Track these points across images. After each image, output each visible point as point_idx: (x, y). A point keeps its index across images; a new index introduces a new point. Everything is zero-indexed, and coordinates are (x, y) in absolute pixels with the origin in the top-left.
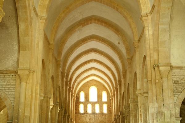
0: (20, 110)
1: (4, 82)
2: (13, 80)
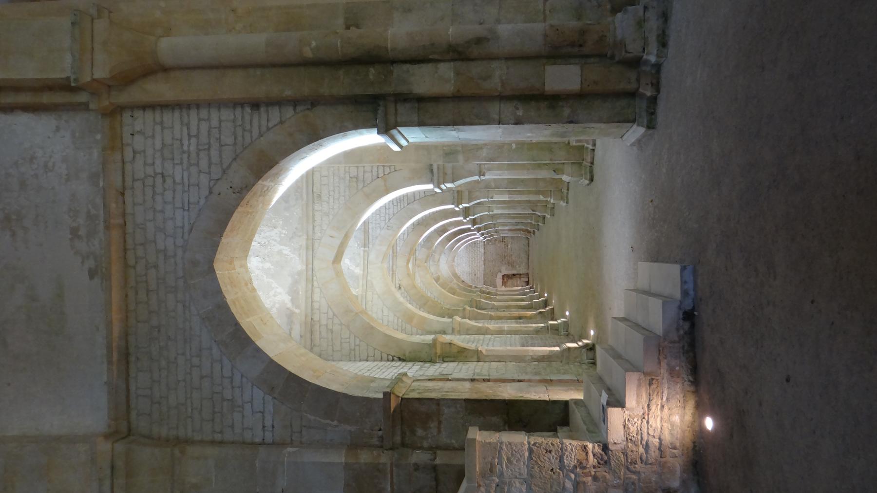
0: (314, 44)
1: (169, 181)
2: (158, 128)
